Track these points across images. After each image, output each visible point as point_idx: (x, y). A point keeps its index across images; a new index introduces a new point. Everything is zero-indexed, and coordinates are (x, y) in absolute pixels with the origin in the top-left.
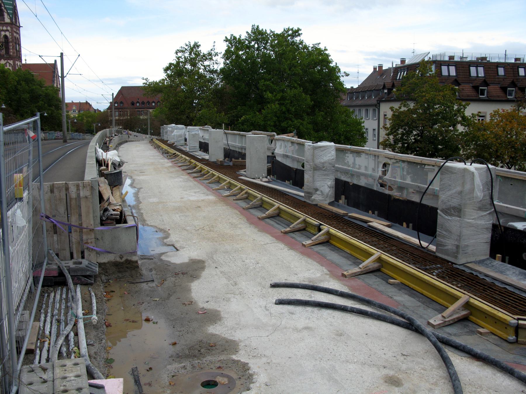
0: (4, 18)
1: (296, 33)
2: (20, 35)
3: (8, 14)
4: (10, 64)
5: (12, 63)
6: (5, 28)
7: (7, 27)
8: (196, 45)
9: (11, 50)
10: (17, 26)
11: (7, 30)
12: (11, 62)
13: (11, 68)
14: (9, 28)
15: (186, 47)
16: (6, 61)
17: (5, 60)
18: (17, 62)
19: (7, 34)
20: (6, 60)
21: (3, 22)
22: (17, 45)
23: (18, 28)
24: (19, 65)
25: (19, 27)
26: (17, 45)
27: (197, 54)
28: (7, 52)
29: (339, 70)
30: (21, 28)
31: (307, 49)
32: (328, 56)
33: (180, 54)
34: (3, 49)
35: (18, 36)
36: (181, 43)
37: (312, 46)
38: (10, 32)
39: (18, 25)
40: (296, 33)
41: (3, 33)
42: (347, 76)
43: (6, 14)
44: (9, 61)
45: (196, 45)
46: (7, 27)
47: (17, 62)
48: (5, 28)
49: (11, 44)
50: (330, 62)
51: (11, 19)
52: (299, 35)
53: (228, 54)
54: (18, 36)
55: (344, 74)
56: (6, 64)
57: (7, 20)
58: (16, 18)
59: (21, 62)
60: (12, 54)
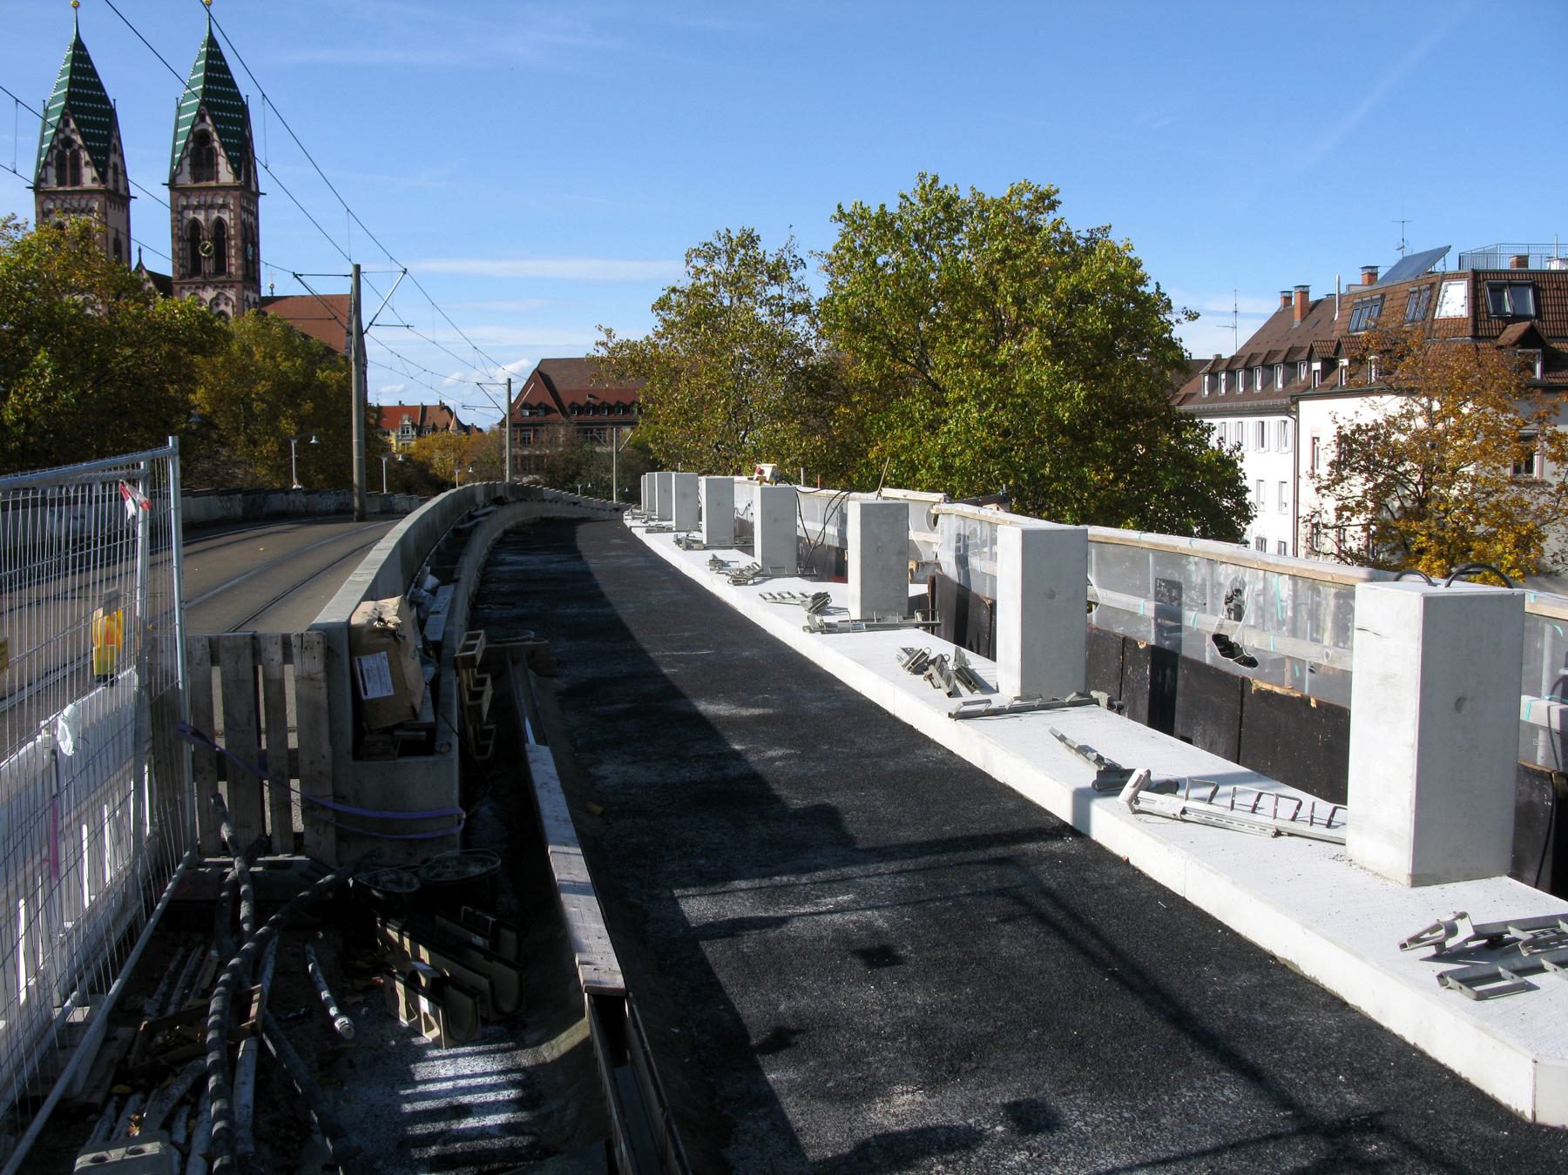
0: (218, 172)
1: (1046, 201)
2: (257, 219)
3: (231, 160)
4: (228, 299)
8: (750, 240)
9: (233, 261)
10: (253, 192)
11: (224, 206)
12: (231, 294)
15: (719, 245)
17: (216, 287)
18: (246, 293)
19: (226, 216)
21: (213, 184)
22: (249, 245)
23: (252, 197)
24: (251, 300)
25: (257, 194)
26: (249, 245)
27: (754, 264)
28: (221, 268)
29: (1169, 306)
30: (262, 199)
31: (1073, 244)
32: (1135, 265)
33: (701, 263)
35: (251, 219)
36: (705, 234)
37: (1087, 235)
39: (254, 189)
40: (1046, 201)
41: (215, 214)
42: (1196, 318)
43: (222, 161)
45: (750, 240)
49: (233, 243)
50: (1142, 281)
51: (237, 174)
52: (1053, 206)
53: (838, 265)
54: (251, 219)
55: (1182, 317)
56: (217, 298)
57: (225, 175)
58: (250, 172)
59: (258, 291)
60: (233, 269)
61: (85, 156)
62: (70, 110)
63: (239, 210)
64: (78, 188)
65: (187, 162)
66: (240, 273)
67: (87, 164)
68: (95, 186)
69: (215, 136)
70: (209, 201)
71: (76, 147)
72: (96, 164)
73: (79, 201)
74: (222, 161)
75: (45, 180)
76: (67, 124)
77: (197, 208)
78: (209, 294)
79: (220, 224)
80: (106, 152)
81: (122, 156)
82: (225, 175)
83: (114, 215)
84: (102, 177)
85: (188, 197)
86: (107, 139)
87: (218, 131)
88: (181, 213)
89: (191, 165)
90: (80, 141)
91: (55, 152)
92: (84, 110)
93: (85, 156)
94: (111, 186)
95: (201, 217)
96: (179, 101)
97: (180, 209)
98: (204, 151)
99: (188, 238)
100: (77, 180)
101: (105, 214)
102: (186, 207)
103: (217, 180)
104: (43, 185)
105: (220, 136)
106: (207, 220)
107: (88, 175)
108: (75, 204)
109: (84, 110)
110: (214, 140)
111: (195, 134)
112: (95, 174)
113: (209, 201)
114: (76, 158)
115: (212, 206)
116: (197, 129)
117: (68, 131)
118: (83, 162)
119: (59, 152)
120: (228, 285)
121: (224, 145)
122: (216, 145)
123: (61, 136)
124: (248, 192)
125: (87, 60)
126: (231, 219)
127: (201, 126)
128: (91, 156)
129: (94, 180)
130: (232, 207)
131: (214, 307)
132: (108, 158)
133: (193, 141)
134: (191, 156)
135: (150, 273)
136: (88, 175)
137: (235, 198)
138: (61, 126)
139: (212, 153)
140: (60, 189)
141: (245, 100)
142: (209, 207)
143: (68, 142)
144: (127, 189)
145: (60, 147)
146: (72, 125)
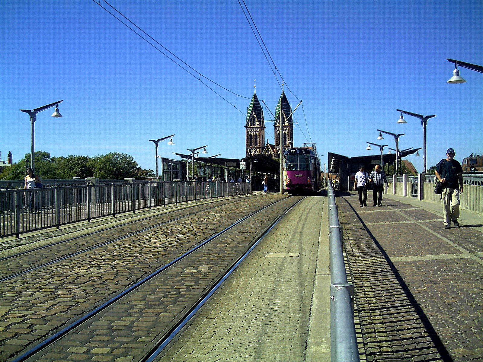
19: (286, 132)
60: (288, 144)
61: (256, 120)
62: (254, 109)
64: (255, 126)
69: (284, 115)
76: (253, 113)
80: (261, 119)
82: (286, 124)
83: (262, 132)
86: (260, 115)
87: (285, 113)
90: (256, 117)
92: (256, 110)
93: (256, 120)
94: (261, 125)
99: (277, 137)
100: (254, 125)
109: (256, 110)
112: (258, 124)
114: (254, 119)
122: (284, 116)
124: (291, 126)
125: (257, 98)
135: (269, 145)
140: (251, 127)
141: (290, 106)
143: (253, 117)
144: (264, 126)
146: (254, 113)
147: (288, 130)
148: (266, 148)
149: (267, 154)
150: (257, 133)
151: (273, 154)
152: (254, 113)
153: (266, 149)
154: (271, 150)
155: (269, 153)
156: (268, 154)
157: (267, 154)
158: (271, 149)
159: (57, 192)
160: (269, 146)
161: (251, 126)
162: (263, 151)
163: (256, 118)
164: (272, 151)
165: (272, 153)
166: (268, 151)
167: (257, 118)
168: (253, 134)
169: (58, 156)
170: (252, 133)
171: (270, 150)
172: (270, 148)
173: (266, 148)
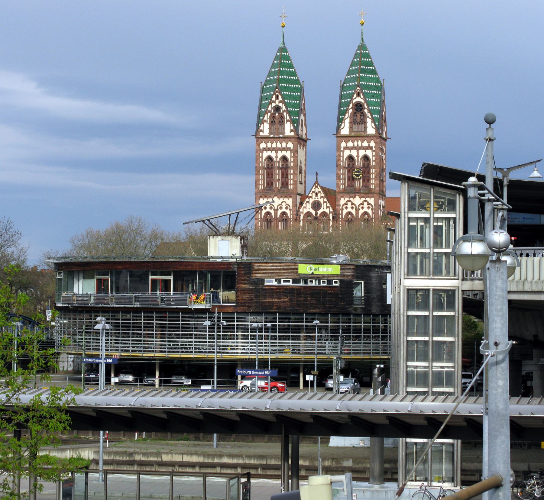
0: (366, 127)
3: (373, 120)
4: (369, 204)
5: (373, 204)
6: (365, 144)
7: (369, 142)
11: (369, 148)
12: (372, 201)
13: (370, 211)
14: (372, 144)
16: (363, 199)
17: (361, 197)
19: (369, 153)
20: (363, 197)
23: (383, 141)
28: (366, 184)
34: (359, 179)
38: (373, 151)
41: (362, 153)
43: (369, 121)
44: (368, 199)
46: (369, 142)
47: (380, 201)
48: (365, 144)
56: (362, 204)
60: (373, 187)
61: (287, 117)
63: (378, 150)
65: (347, 122)
66: (378, 189)
67: (288, 121)
68: (292, 133)
69: (366, 106)
70: (360, 145)
71: (281, 112)
72: (292, 121)
73: (281, 144)
74: (369, 121)
75: (262, 131)
76: (277, 97)
77: (353, 148)
78: (358, 201)
79: (366, 158)
80: (298, 114)
81: (305, 115)
82: (371, 130)
84: (296, 130)
85: (347, 143)
88: (343, 151)
89: (350, 123)
90: (284, 108)
91: (269, 114)
92: (286, 89)
93: (287, 117)
95: (354, 153)
96: (342, 82)
97: (342, 149)
98: (359, 115)
101: (297, 151)
102: (346, 148)
103: (365, 131)
104: (261, 134)
105: (368, 106)
106: (358, 156)
107: (288, 129)
108: (279, 145)
109: (286, 89)
110: (365, 108)
111: (353, 105)
112: (292, 128)
113: (360, 145)
114: (282, 117)
115: (362, 148)
116: (354, 101)
117: (277, 101)
118: (285, 120)
119: (271, 114)
120: (370, 195)
121: (370, 111)
122: (366, 111)
123: (273, 105)
126: (373, 156)
127: (358, 99)
128: (290, 117)
129: (291, 131)
130: (374, 149)
131: (361, 209)
132: (299, 117)
133: (352, 108)
134: (351, 117)
136: (288, 129)
137: (376, 143)
138: (274, 99)
139: (363, 114)
140: (271, 136)
141: (382, 82)
142: (358, 149)
145: (272, 112)
146: (280, 98)
147: (374, 149)
148: (311, 197)
149: (313, 212)
150: (288, 154)
151: (330, 212)
152: (280, 98)
153: (311, 201)
154: (325, 202)
155: (319, 212)
156: (316, 213)
157: (313, 212)
158: (325, 200)
159: (498, 186)
160: (320, 190)
161: (270, 133)
162: (301, 203)
163: (284, 111)
164: (328, 205)
165: (327, 211)
166: (316, 205)
167: (289, 113)
168: (277, 157)
169: (422, 166)
170: (273, 154)
171: (322, 201)
172: (321, 197)
173: (311, 197)
